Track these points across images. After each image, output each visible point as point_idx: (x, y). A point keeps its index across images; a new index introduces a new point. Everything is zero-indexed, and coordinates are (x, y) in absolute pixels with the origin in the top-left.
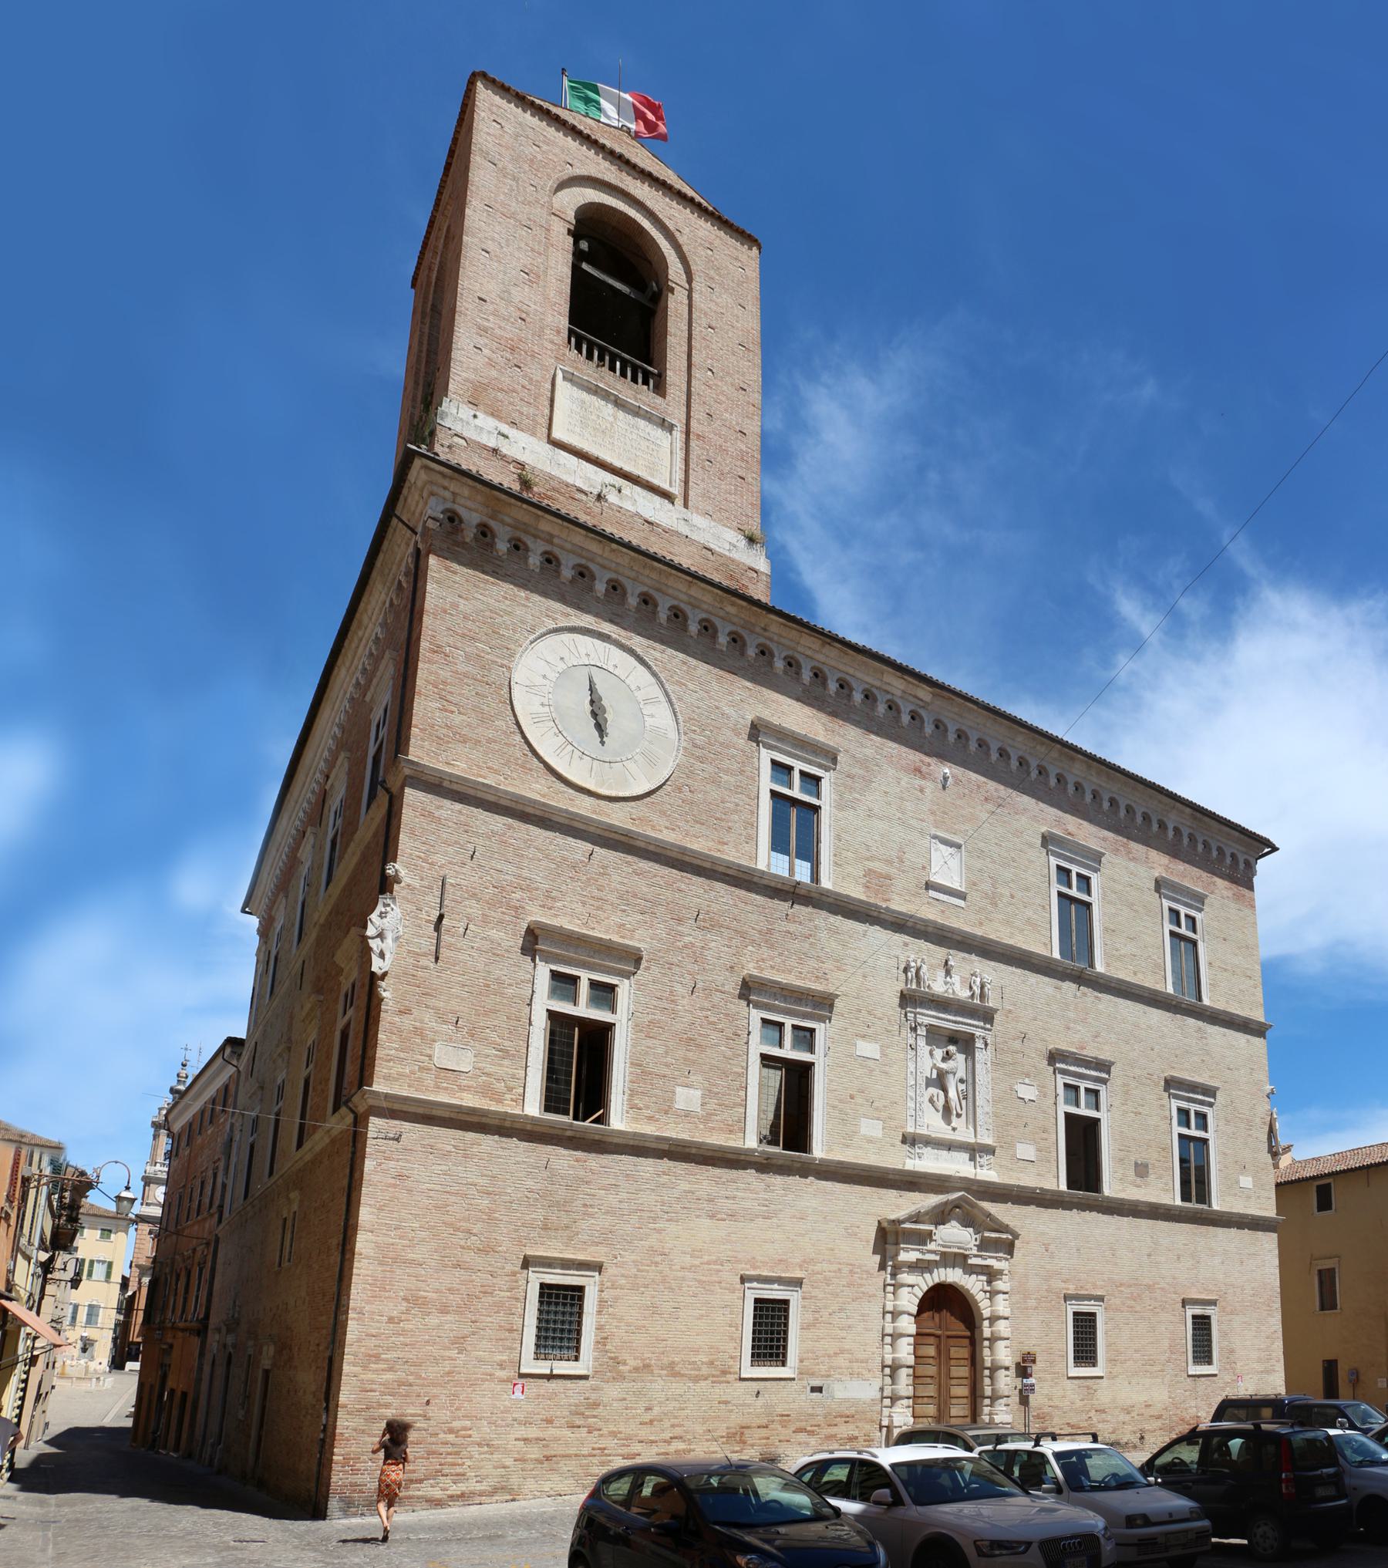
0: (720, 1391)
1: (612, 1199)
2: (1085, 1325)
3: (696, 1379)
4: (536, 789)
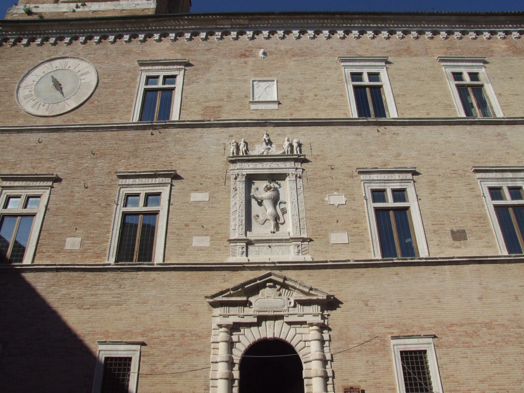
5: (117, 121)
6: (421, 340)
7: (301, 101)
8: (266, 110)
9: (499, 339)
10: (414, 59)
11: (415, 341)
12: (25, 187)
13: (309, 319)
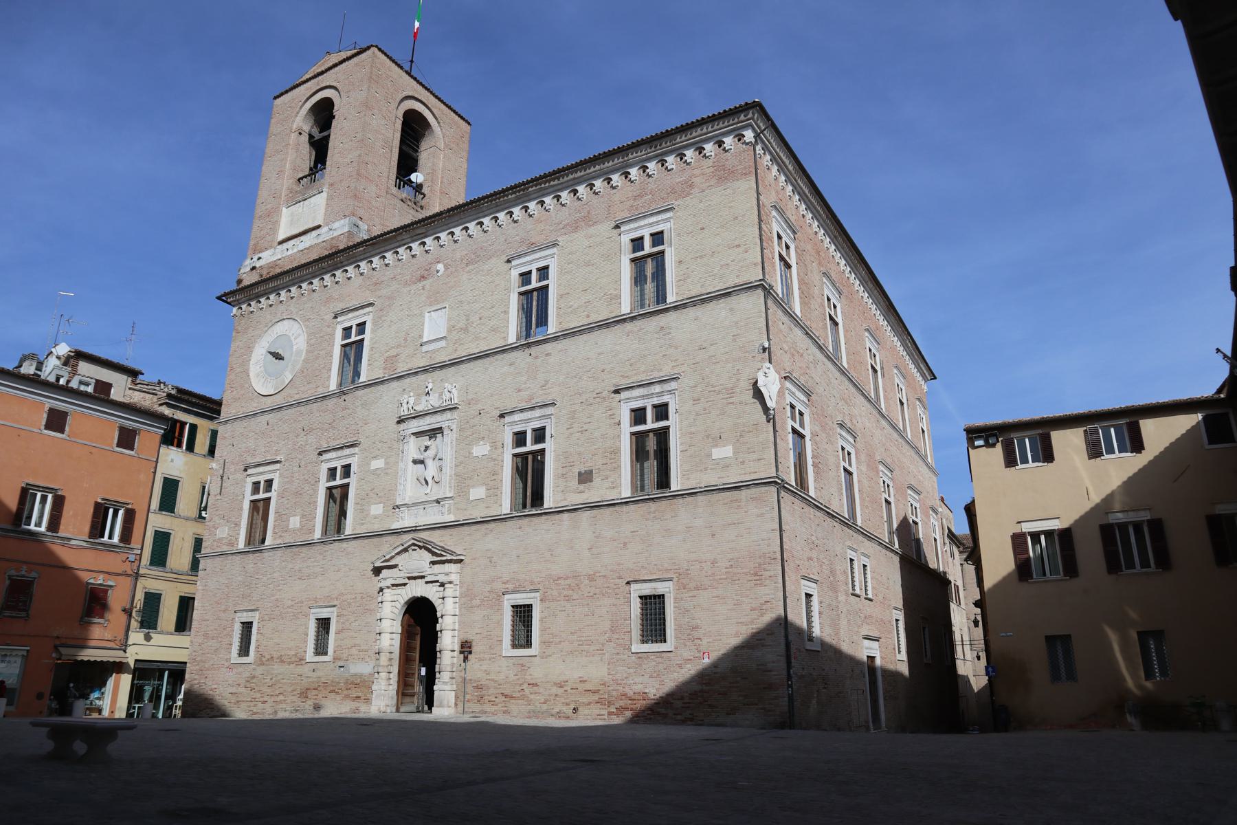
0: (299, 670)
1: (265, 579)
2: (523, 614)
3: (290, 663)
4: (253, 407)
5: (321, 391)
6: (529, 595)
7: (466, 330)
8: (434, 351)
9: (598, 591)
10: (592, 230)
11: (524, 595)
12: (261, 473)
13: (442, 578)
